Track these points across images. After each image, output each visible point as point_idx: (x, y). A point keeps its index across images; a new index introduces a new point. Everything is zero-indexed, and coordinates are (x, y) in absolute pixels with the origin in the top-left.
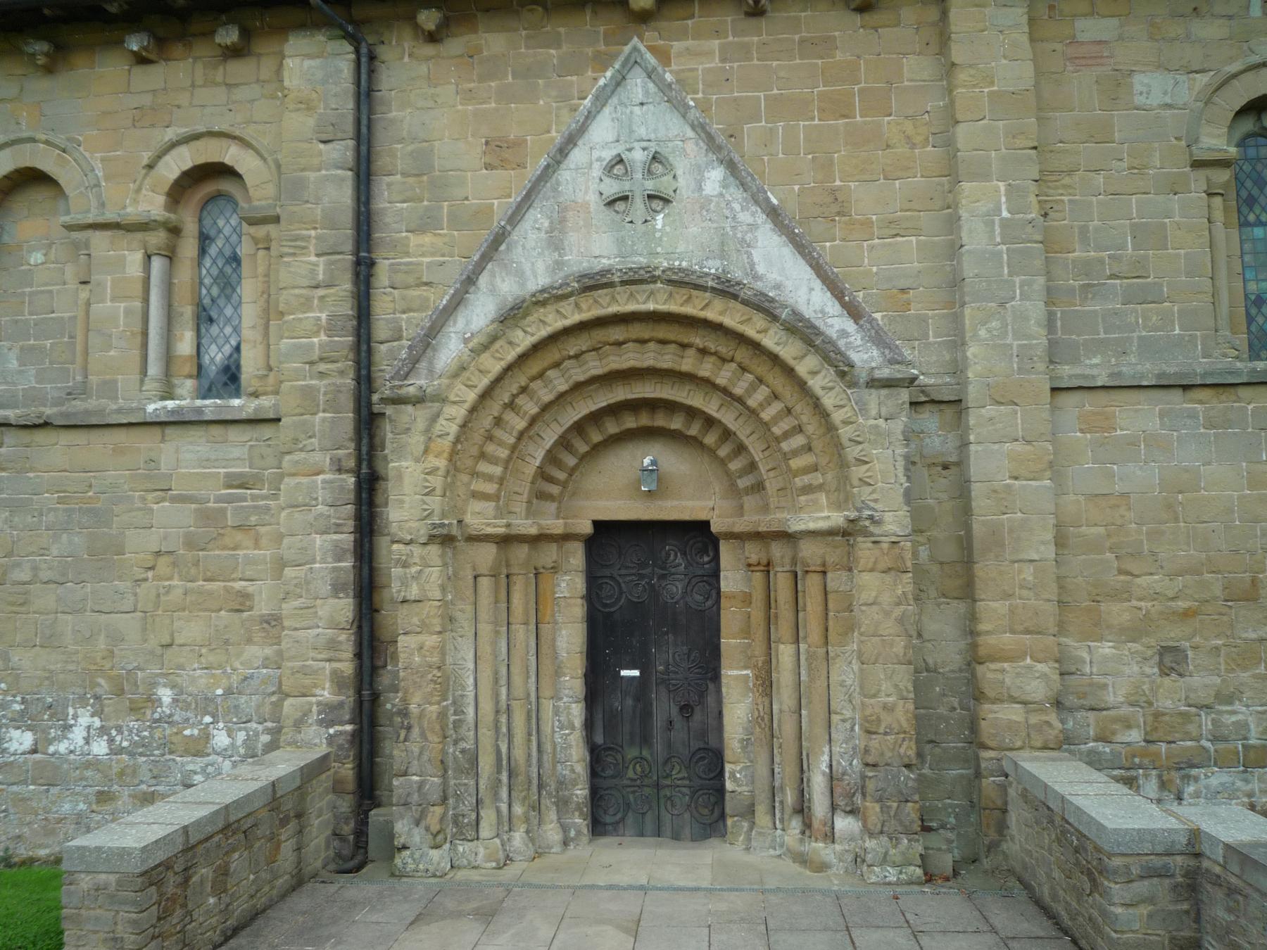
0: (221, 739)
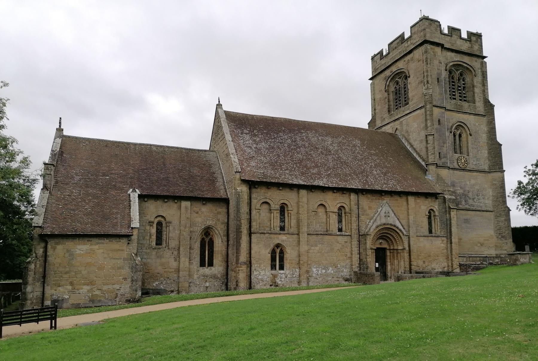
0: (345, 270)
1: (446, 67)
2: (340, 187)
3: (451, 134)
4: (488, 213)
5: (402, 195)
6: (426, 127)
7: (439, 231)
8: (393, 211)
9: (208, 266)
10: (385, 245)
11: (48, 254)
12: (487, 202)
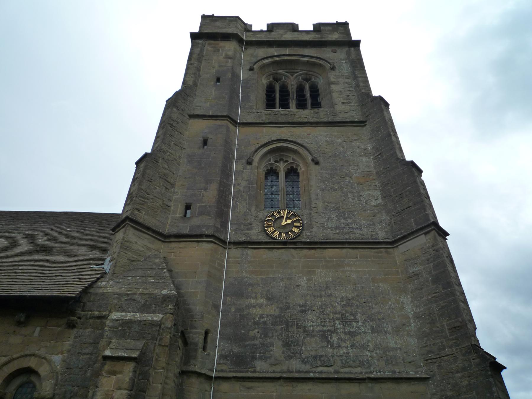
4: (404, 387)
12: (392, 341)
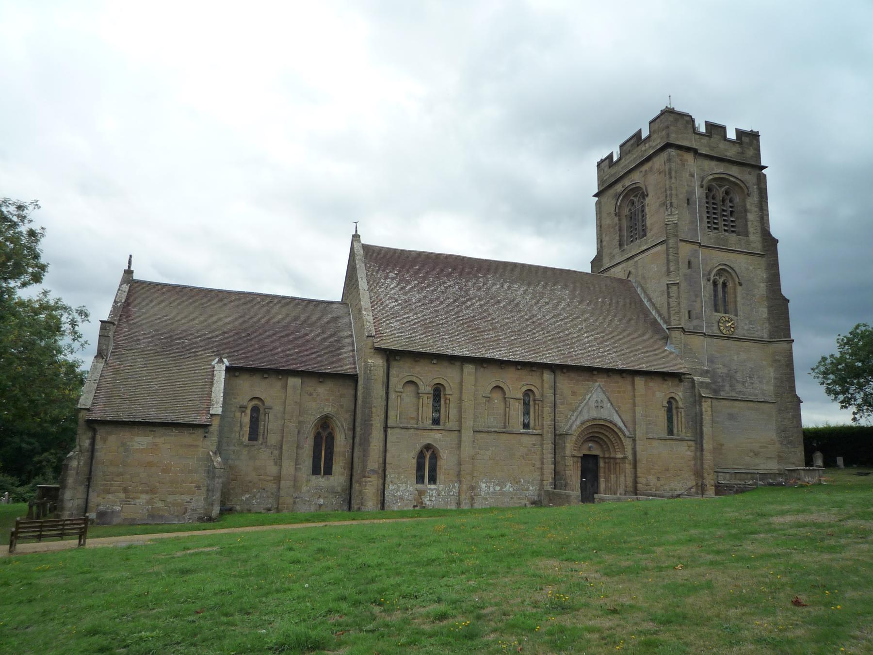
0: (531, 488)
1: (702, 182)
2: (526, 360)
3: (708, 283)
4: (767, 405)
5: (624, 375)
6: (668, 272)
7: (684, 431)
8: (609, 400)
9: (325, 474)
10: (597, 451)
11: (97, 447)
12: (765, 387)
